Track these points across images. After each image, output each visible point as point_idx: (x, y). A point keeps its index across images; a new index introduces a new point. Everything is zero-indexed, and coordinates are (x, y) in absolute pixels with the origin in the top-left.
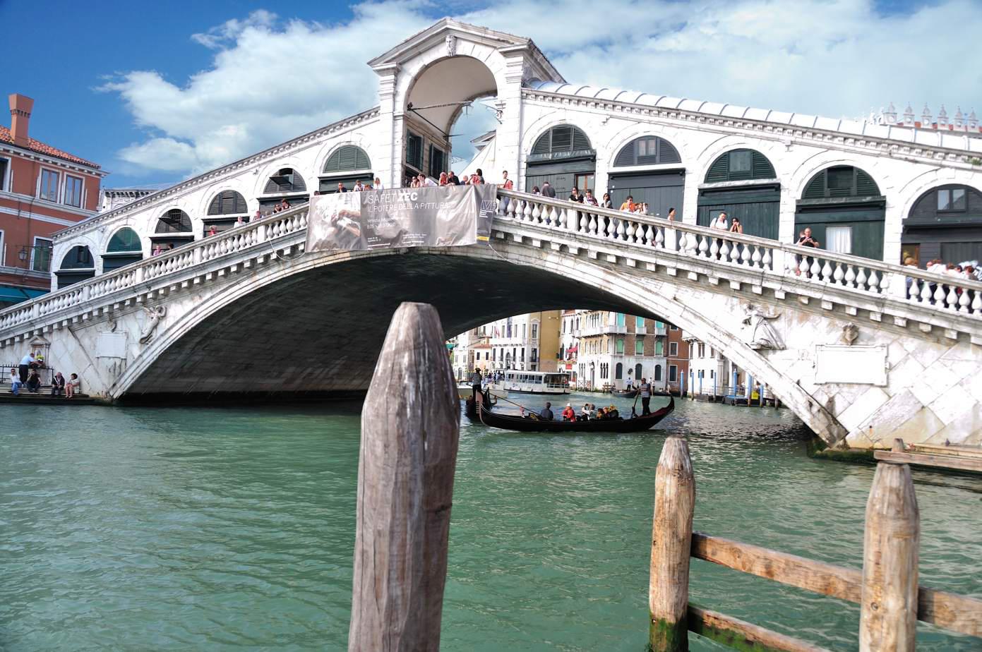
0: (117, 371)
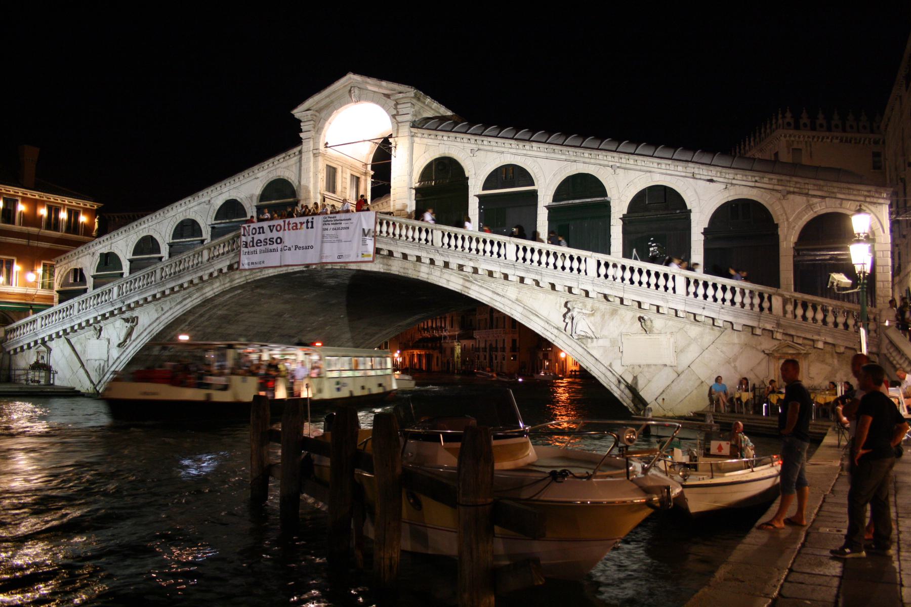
0: (102, 372)
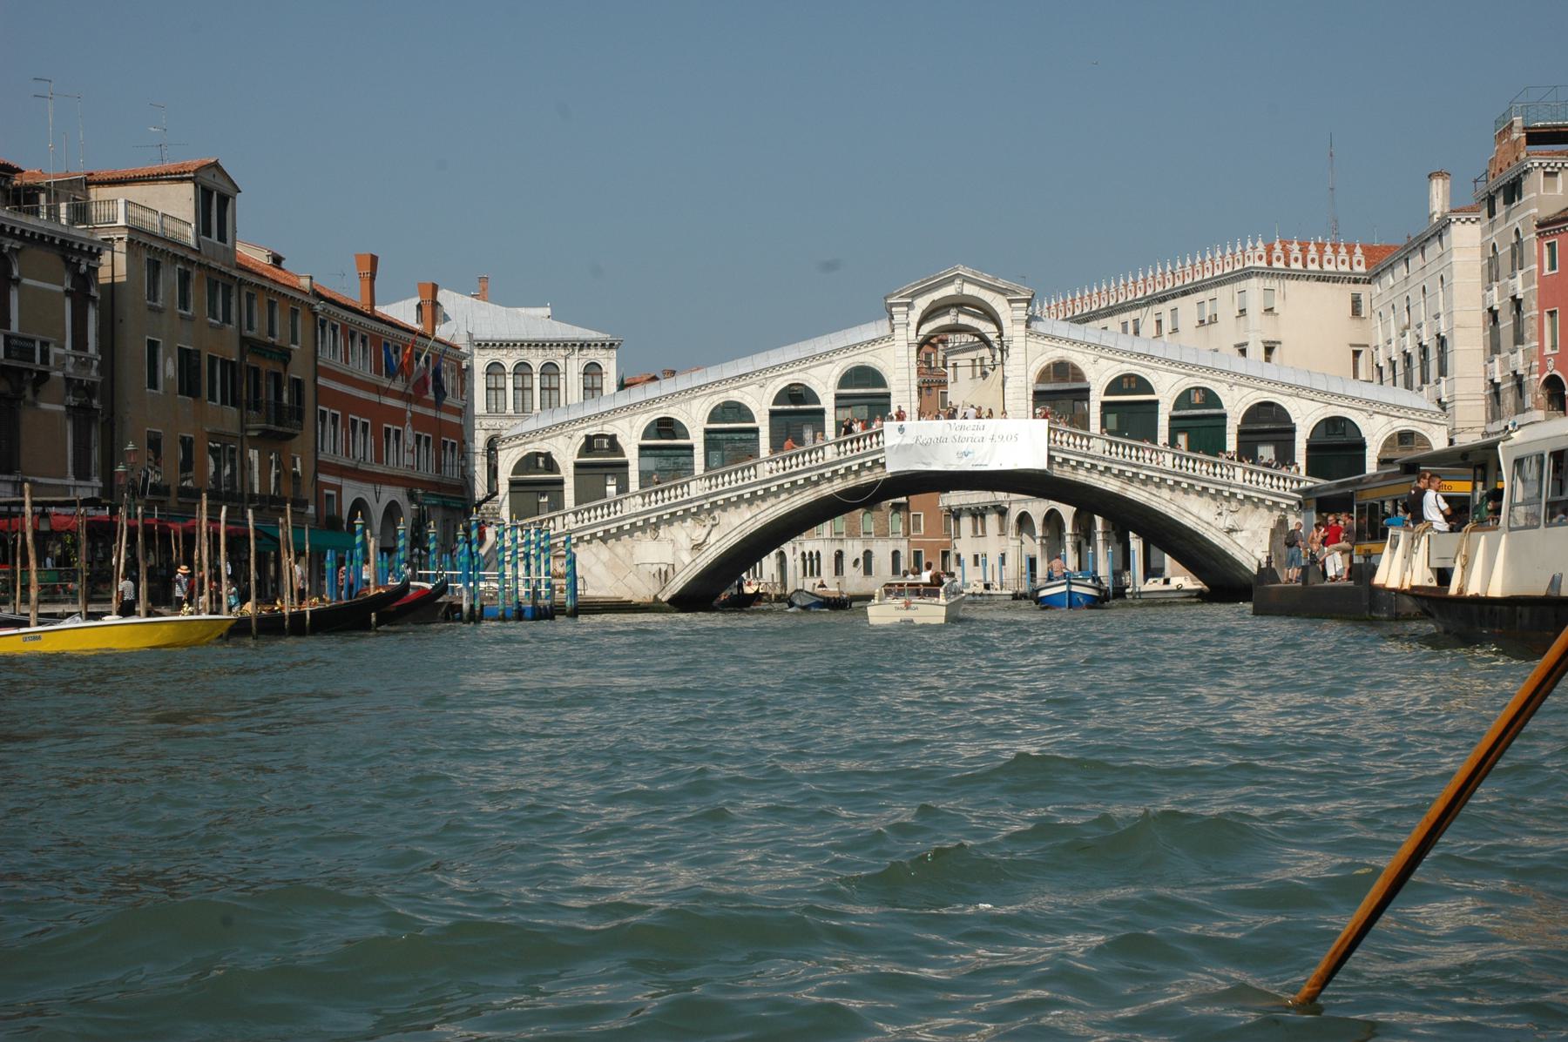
0: (664, 577)
